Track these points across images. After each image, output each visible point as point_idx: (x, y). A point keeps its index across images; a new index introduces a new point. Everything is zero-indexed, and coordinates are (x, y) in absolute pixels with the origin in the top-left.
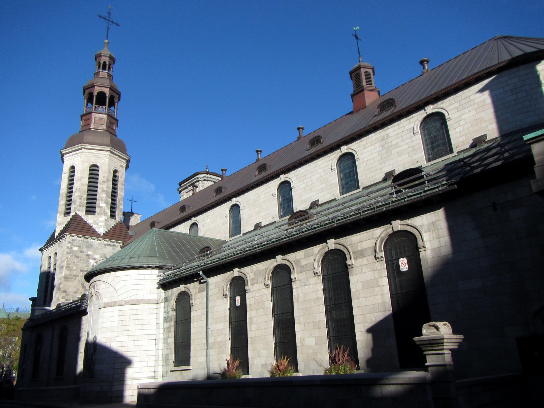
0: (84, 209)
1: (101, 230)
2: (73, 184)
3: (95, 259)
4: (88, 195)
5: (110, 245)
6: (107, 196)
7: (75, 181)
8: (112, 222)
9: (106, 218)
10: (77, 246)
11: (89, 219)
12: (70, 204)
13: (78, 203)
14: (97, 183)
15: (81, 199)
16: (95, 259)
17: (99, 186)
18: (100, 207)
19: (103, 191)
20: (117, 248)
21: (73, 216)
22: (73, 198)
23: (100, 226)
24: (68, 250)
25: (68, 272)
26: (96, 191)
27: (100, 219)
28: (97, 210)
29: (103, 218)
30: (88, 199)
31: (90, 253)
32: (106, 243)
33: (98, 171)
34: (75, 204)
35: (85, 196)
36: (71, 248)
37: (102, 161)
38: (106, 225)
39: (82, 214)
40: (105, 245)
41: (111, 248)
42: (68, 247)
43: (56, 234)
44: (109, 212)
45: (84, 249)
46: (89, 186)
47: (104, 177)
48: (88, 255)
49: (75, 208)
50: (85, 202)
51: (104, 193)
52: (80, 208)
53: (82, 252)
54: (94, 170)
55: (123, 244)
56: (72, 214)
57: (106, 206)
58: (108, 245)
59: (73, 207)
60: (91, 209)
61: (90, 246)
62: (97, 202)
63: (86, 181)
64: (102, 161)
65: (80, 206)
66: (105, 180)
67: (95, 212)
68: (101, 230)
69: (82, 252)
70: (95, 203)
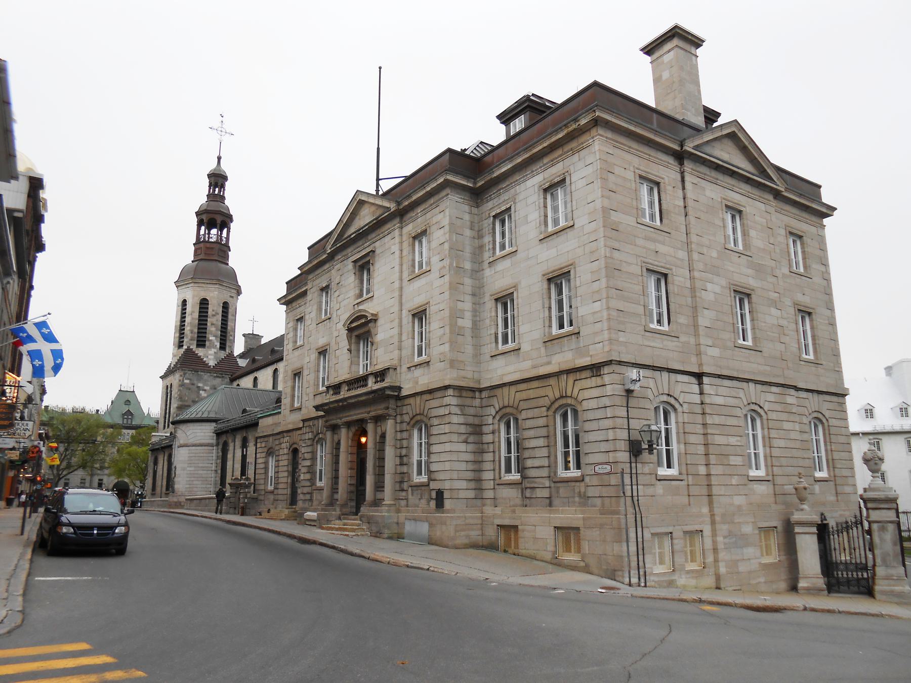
0: (195, 342)
1: (212, 363)
2: (185, 317)
3: (205, 390)
4: (199, 328)
5: (220, 377)
6: (217, 330)
7: (187, 315)
8: (222, 355)
9: (216, 351)
10: (188, 379)
11: (200, 352)
12: (183, 337)
13: (189, 337)
14: (207, 316)
15: (192, 333)
16: (205, 390)
17: (209, 320)
18: (210, 341)
19: (212, 324)
20: (226, 380)
21: (186, 349)
22: (185, 331)
23: (210, 359)
24: (180, 383)
25: (181, 403)
26: (206, 324)
27: (210, 352)
28: (207, 343)
29: (212, 351)
30: (198, 332)
31: (200, 385)
32: (215, 375)
33: (208, 304)
34: (187, 338)
35: (196, 330)
36: (183, 381)
37: (212, 295)
38: (216, 358)
39: (193, 347)
40: (215, 377)
41: (220, 379)
42: (180, 380)
43: (172, 366)
44: (218, 345)
45: (195, 382)
46: (199, 320)
47: (213, 311)
48: (198, 387)
49: (187, 342)
50: (196, 336)
51: (213, 326)
52: (192, 342)
53: (193, 384)
54: (204, 303)
55: (232, 375)
56: (185, 347)
57: (216, 339)
58: (217, 377)
59: (185, 340)
60: (201, 342)
61: (200, 379)
62: (207, 336)
63: (196, 315)
64: (212, 295)
65: (191, 340)
66: (214, 313)
67: (205, 345)
68: (212, 363)
69: (193, 384)
70: (205, 337)
